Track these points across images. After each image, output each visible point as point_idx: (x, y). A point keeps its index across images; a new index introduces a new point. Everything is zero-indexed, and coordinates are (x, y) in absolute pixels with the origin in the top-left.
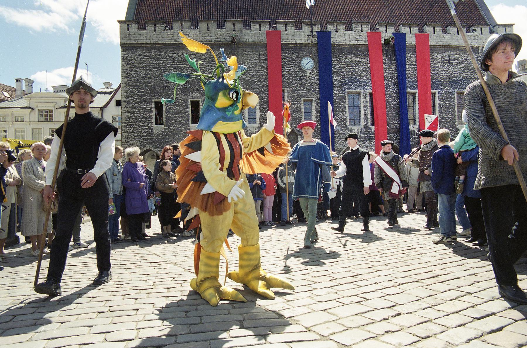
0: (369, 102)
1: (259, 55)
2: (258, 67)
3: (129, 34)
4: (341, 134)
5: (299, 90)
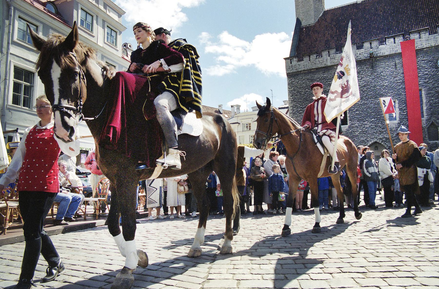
1: (395, 64)
2: (395, 73)
3: (292, 66)
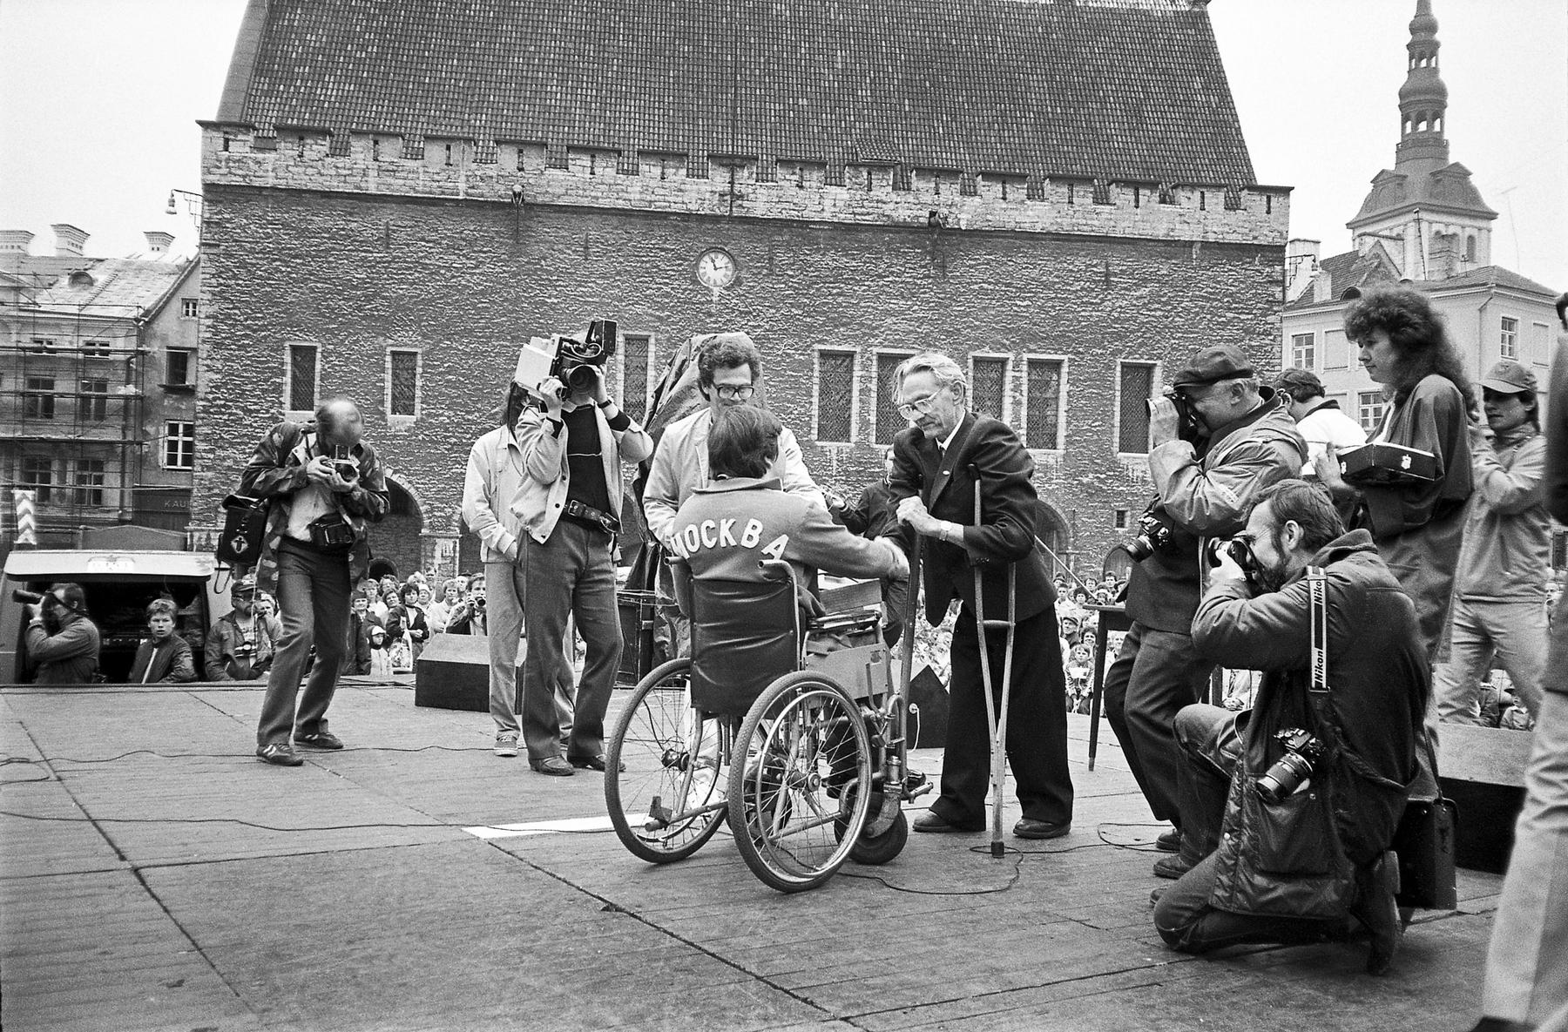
0: (875, 381)
1: (587, 241)
3: (228, 160)
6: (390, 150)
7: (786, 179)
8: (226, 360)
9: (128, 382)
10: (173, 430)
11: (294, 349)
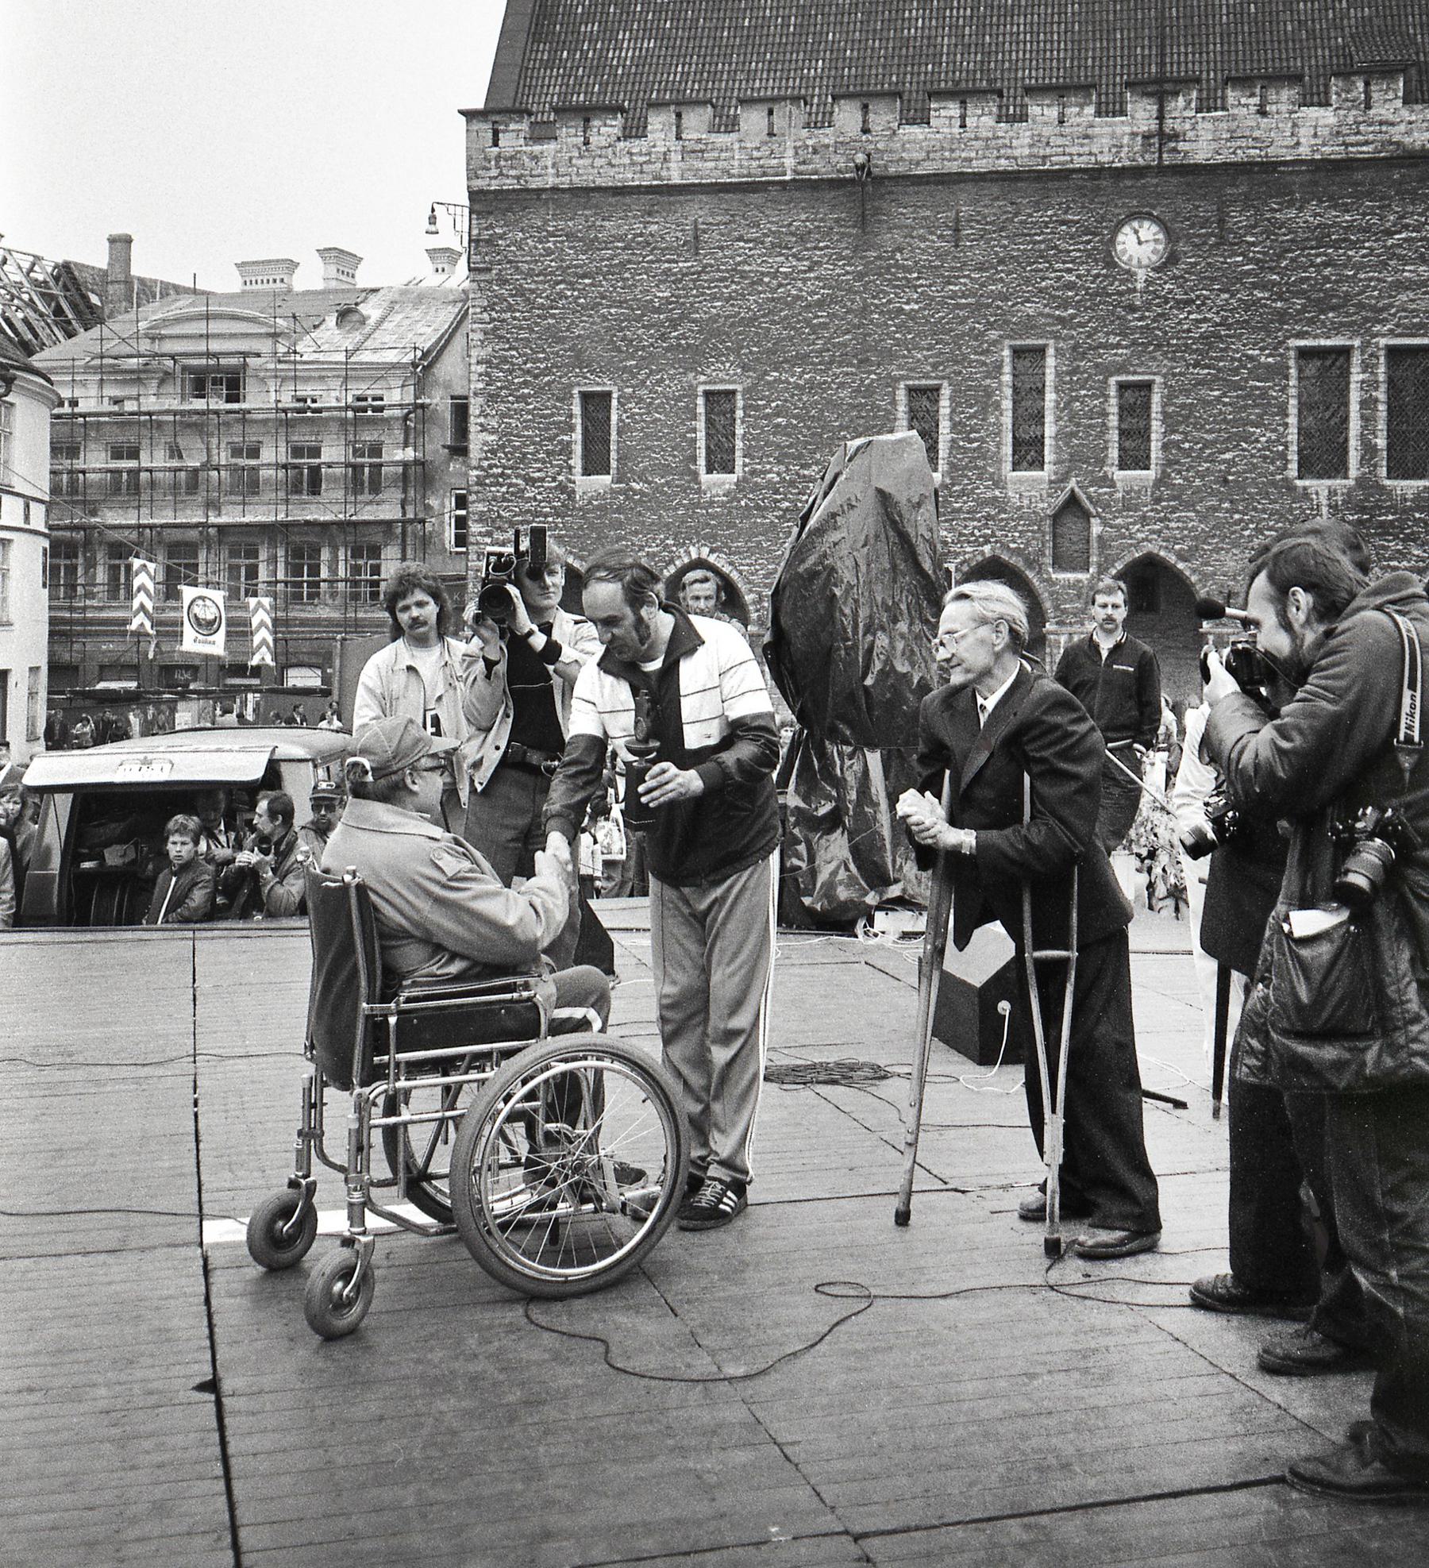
1: (957, 220)
3: (498, 157)
4: (1264, 511)
5: (1101, 346)
6: (696, 121)
7: (1241, 104)
8: (503, 416)
9: (406, 445)
10: (461, 502)
11: (586, 397)
